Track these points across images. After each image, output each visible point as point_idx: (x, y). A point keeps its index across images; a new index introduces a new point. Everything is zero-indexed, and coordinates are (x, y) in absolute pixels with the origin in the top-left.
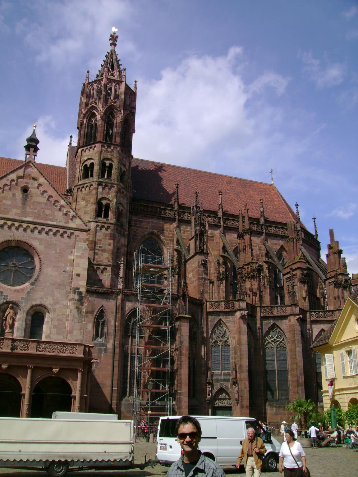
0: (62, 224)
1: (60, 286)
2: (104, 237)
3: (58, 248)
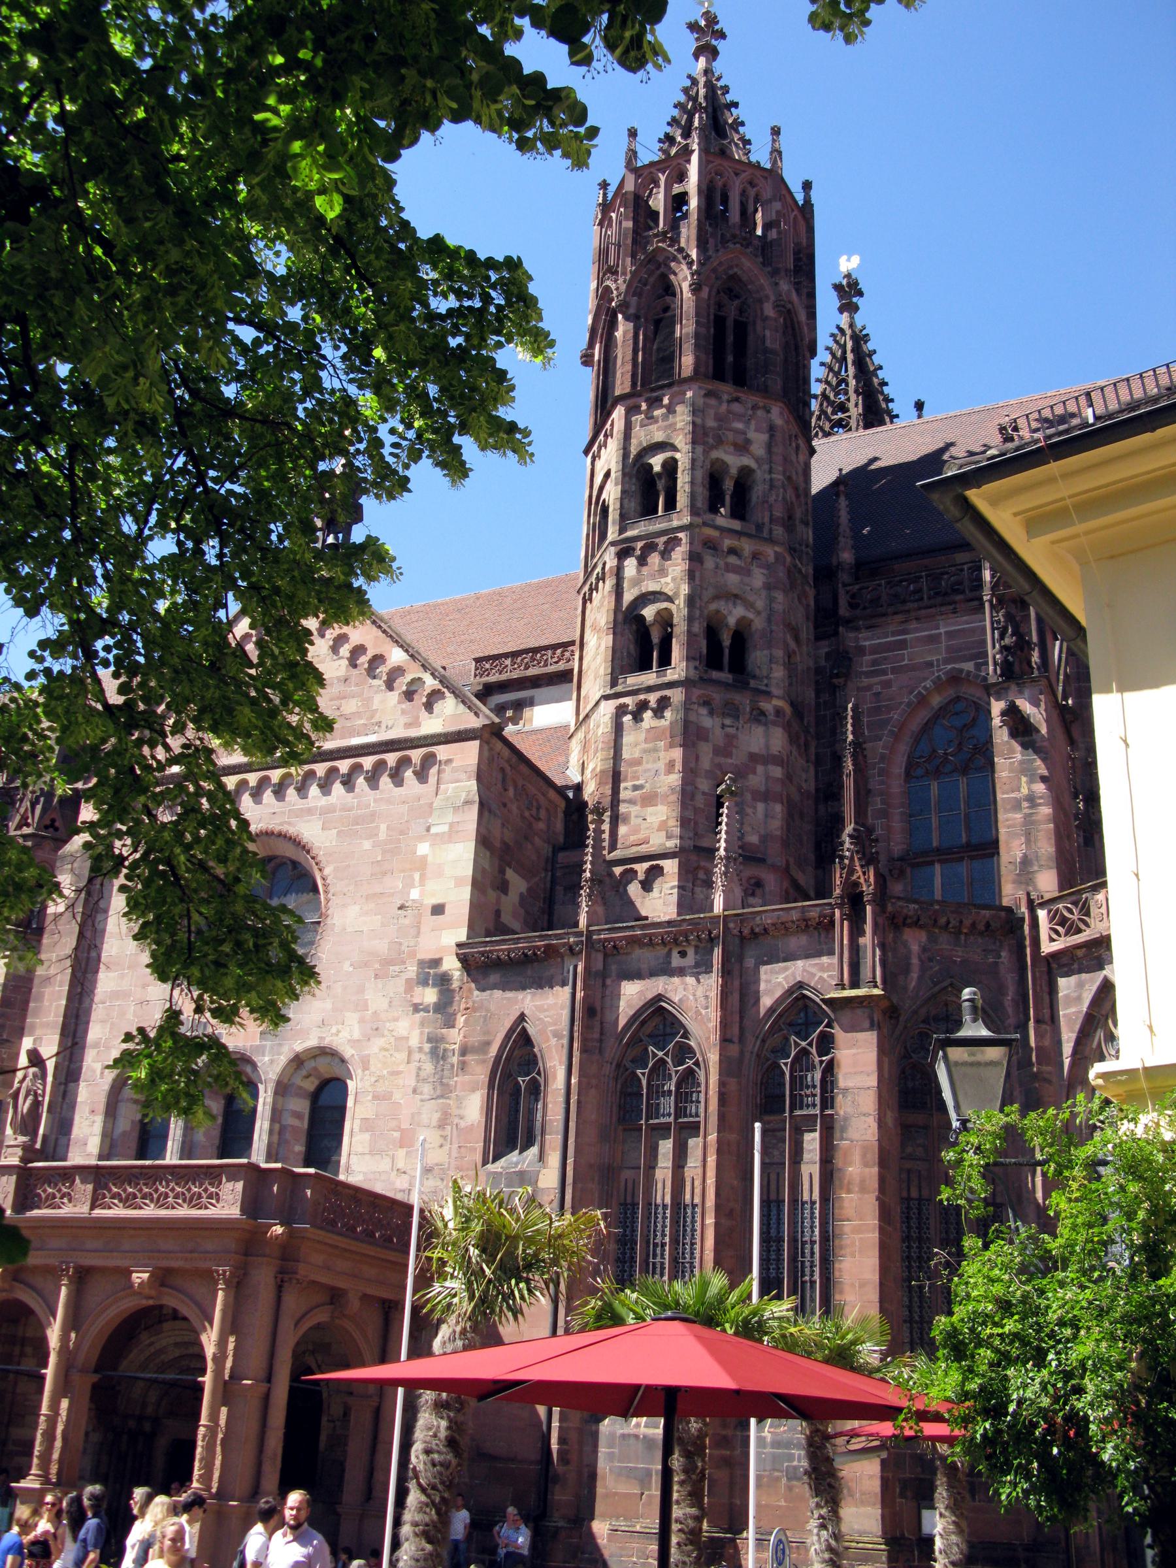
0: (398, 732)
1: (385, 966)
2: (651, 745)
3: (383, 827)
